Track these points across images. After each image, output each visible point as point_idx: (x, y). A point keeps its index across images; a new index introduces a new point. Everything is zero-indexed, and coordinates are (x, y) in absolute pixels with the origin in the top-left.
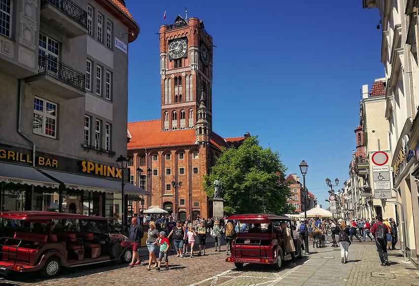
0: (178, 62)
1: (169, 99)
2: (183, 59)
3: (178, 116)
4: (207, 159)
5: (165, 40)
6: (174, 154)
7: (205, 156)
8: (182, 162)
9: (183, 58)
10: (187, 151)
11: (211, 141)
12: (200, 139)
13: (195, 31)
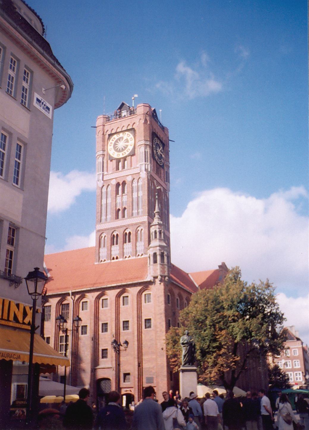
2: (129, 158)
3: (120, 240)
4: (166, 303)
6: (114, 298)
9: (129, 156)
11: (171, 275)
13: (146, 121)
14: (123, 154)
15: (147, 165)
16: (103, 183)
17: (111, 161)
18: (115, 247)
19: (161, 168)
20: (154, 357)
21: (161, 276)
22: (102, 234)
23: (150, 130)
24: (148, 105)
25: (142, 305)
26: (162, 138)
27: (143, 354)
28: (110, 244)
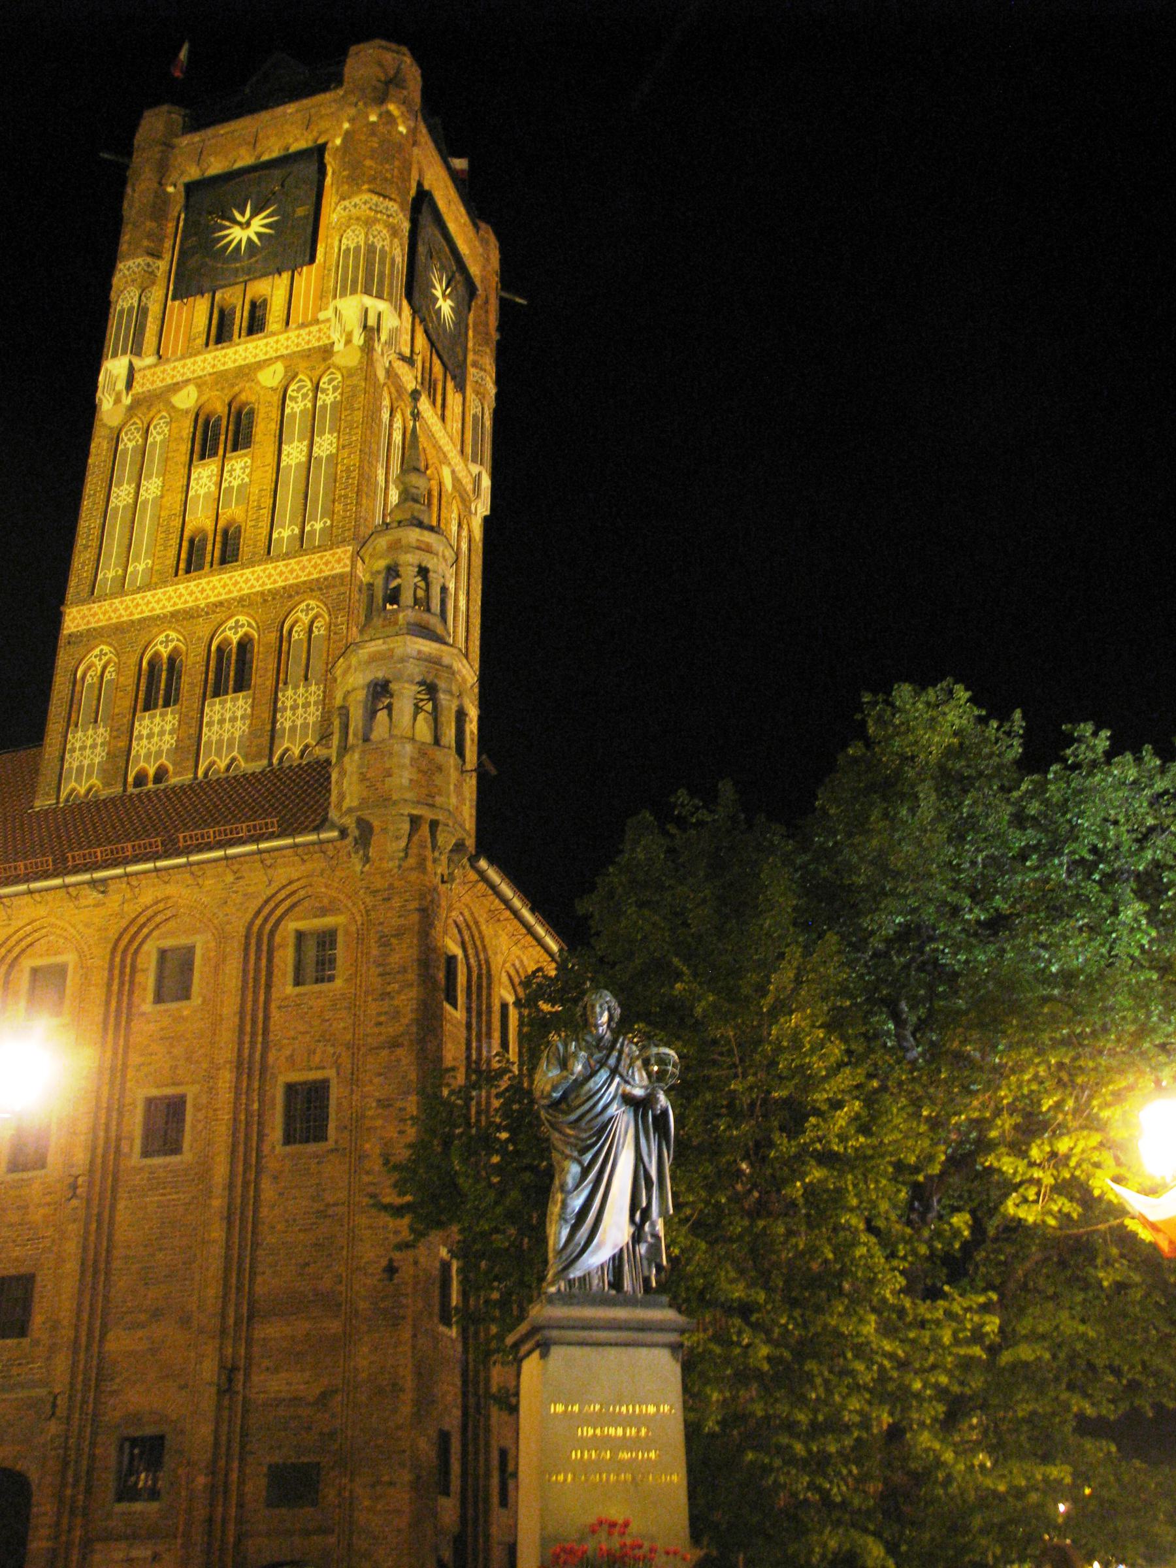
18: (158, 719)
20: (334, 1326)
25: (275, 994)
28: (127, 703)
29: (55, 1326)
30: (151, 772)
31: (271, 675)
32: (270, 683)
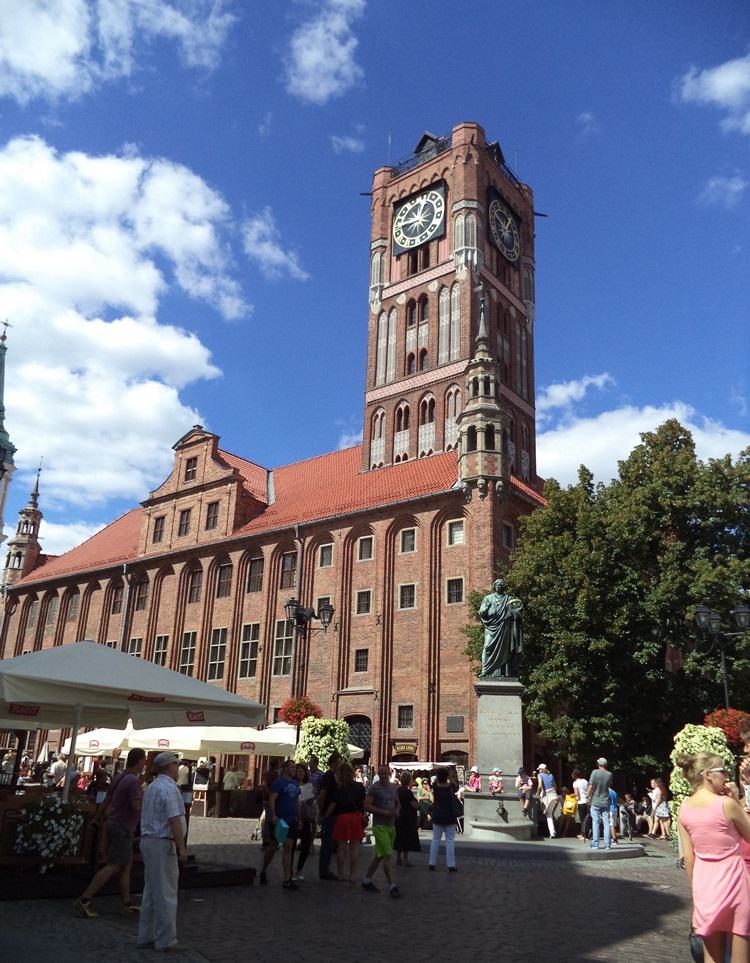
0: (420, 254)
1: (388, 367)
5: (383, 205)
6: (382, 535)
7: (487, 531)
8: (409, 563)
10: (425, 518)
11: (513, 480)
12: (470, 468)
13: (469, 157)
14: (421, 239)
15: (470, 253)
16: (382, 306)
17: (398, 257)
19: (512, 270)
21: (487, 479)
22: (376, 410)
23: (480, 180)
24: (475, 126)
25: (443, 548)
26: (515, 204)
27: (442, 660)
28: (391, 430)
29: (376, 667)
30: (401, 456)
31: (442, 416)
32: (441, 419)
